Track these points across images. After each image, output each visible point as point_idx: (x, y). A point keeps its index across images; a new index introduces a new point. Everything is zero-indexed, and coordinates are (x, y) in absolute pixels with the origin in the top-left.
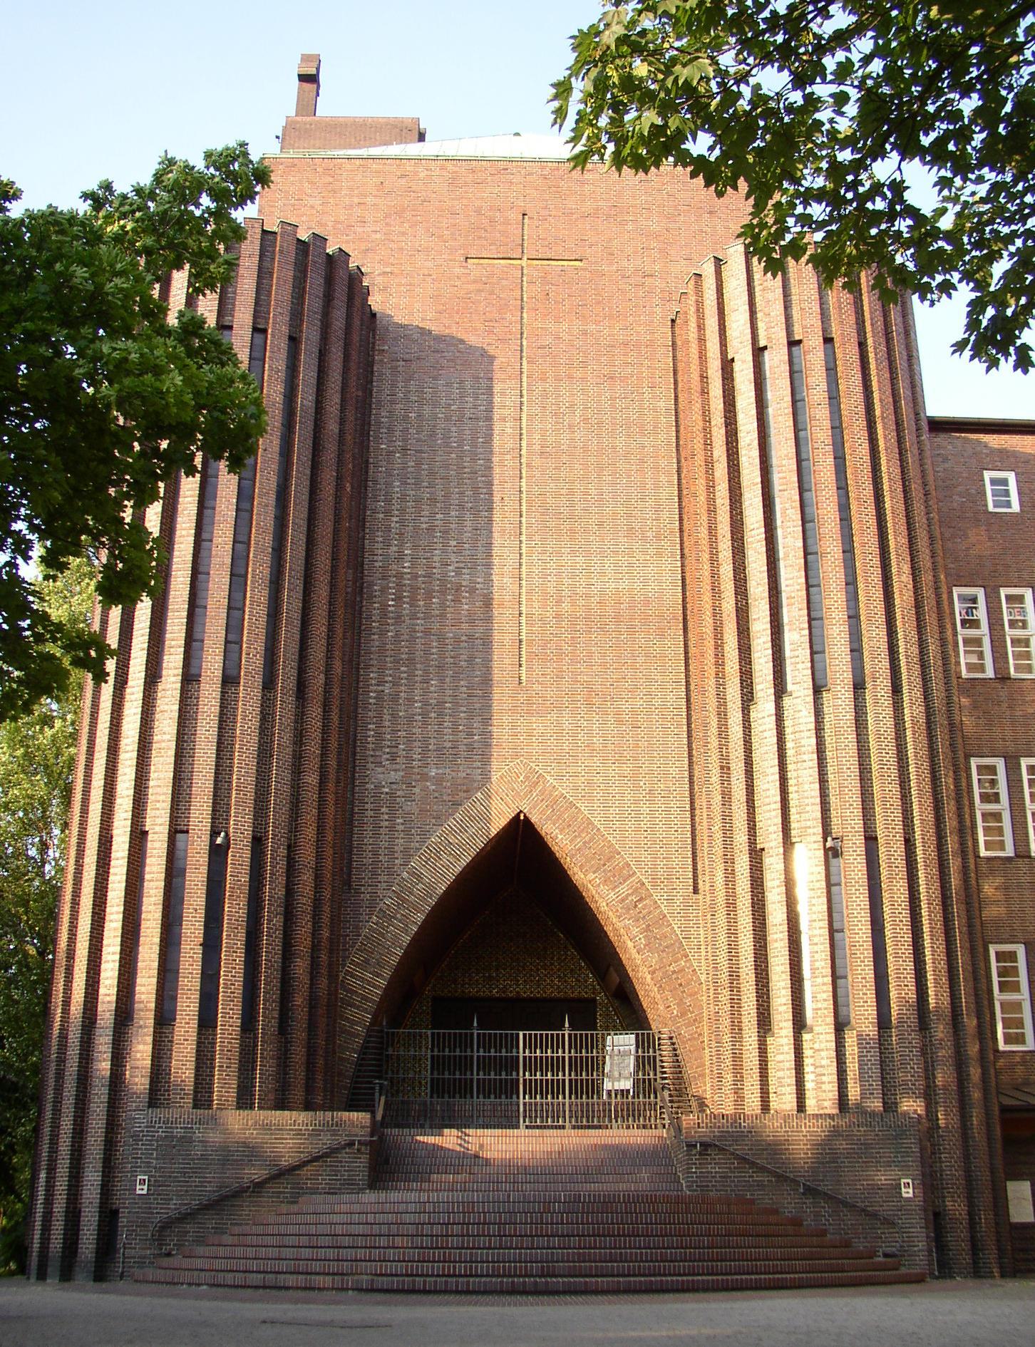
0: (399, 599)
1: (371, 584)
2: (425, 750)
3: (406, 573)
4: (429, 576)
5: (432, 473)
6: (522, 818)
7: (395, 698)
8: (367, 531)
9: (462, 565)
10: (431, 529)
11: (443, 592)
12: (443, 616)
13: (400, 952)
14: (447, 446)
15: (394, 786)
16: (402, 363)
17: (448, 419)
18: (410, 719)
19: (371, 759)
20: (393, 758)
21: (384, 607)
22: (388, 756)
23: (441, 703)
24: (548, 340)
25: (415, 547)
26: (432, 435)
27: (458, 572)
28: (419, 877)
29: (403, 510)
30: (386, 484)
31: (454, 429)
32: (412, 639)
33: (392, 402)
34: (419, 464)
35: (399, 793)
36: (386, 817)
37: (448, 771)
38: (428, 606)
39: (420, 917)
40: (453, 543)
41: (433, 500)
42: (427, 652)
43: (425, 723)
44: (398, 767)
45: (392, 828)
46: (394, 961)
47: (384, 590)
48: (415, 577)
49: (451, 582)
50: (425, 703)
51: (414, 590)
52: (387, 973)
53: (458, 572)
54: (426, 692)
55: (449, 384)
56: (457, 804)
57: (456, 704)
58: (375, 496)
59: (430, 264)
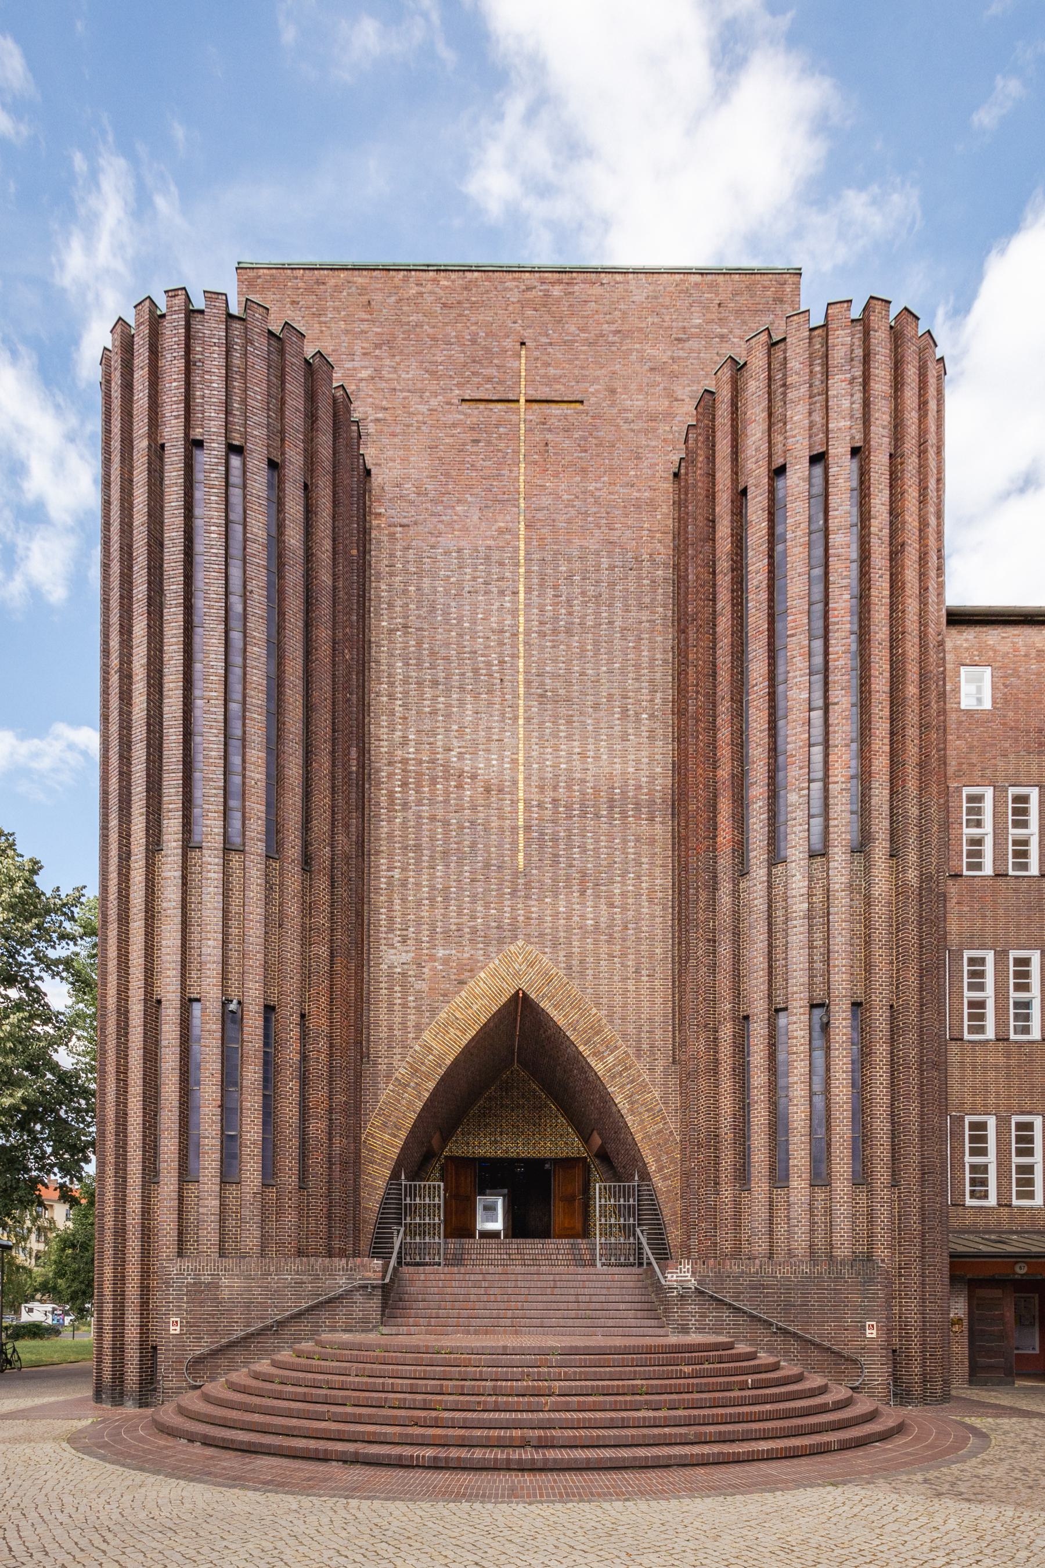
0: (404, 784)
1: (378, 770)
2: (433, 931)
3: (411, 759)
4: (433, 761)
5: (433, 654)
7: (404, 884)
8: (372, 715)
9: (463, 750)
10: (434, 712)
11: (447, 779)
12: (446, 801)
13: (414, 1116)
14: (447, 624)
15: (406, 967)
16: (399, 529)
17: (447, 593)
18: (419, 904)
19: (383, 942)
20: (404, 940)
21: (391, 794)
22: (399, 939)
23: (446, 888)
24: (546, 501)
25: (419, 732)
26: (433, 609)
27: (461, 756)
28: (430, 1049)
29: (406, 693)
30: (389, 665)
31: (453, 604)
32: (419, 826)
33: (391, 574)
34: (419, 644)
35: (410, 973)
36: (399, 995)
38: (433, 792)
39: (431, 1085)
40: (455, 727)
41: (435, 683)
42: (432, 839)
43: (432, 906)
44: (408, 948)
45: (404, 1006)
46: (409, 1124)
47: (390, 776)
48: (420, 762)
49: (454, 768)
50: (432, 888)
51: (419, 774)
52: (403, 1134)
53: (461, 756)
54: (432, 877)
55: (447, 553)
56: (462, 983)
57: (461, 889)
58: (379, 678)
59: (424, 408)
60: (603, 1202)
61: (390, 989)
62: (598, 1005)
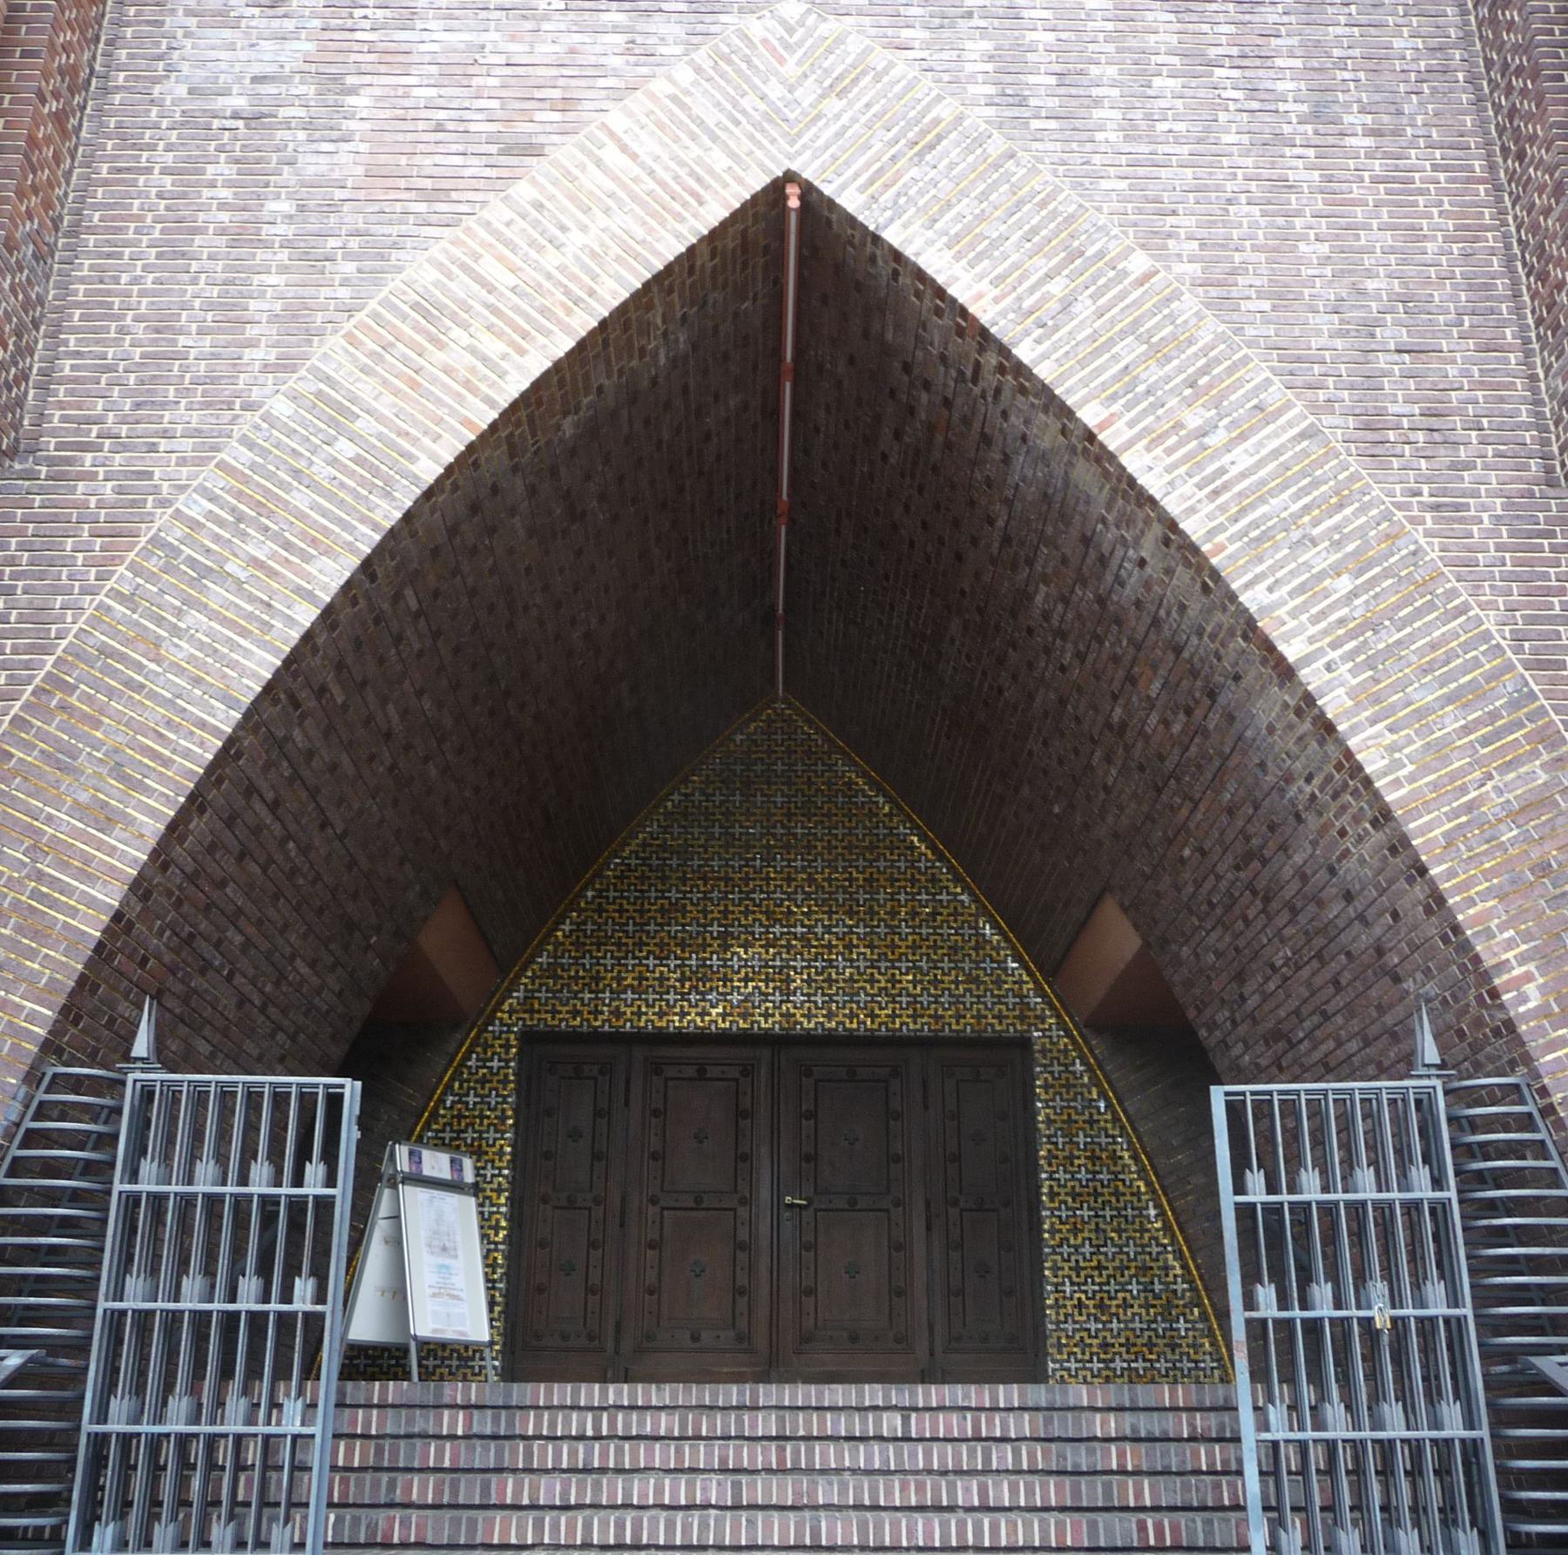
6: (794, 203)
15: (270, 89)
37: (493, 36)
44: (289, 24)
45: (244, 237)
60: (1257, 1194)
61: (189, 171)
62: (1154, 241)
